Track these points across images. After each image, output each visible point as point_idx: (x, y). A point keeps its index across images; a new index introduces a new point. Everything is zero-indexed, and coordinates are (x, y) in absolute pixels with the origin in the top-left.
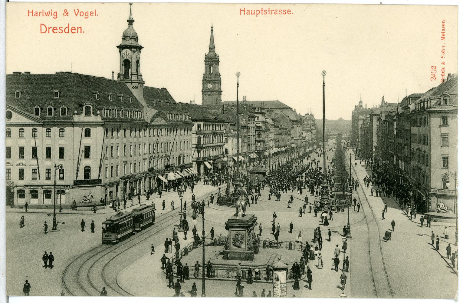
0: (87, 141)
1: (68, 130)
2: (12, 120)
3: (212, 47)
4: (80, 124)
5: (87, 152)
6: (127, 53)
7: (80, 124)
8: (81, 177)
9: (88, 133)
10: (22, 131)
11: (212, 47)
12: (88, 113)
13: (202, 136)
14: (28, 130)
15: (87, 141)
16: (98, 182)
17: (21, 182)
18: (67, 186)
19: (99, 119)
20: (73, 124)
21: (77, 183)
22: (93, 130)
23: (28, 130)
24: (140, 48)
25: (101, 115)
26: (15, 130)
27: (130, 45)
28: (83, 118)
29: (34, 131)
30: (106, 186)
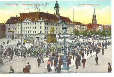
0: (41, 25)
1: (37, 23)
2: (27, 22)
3: (94, 13)
4: (39, 22)
5: (41, 27)
6: (56, 8)
7: (39, 22)
8: (40, 33)
9: (41, 24)
10: (28, 23)
11: (94, 13)
12: (41, 19)
13: (78, 29)
14: (29, 23)
15: (41, 25)
16: (43, 34)
17: (28, 34)
18: (37, 35)
19: (43, 21)
20: (37, 22)
21: (38, 34)
22: (42, 23)
23: (29, 23)
24: (59, 7)
25: (44, 20)
26: (27, 24)
27: (57, 6)
28: (40, 20)
29: (31, 23)
30: (45, 35)
